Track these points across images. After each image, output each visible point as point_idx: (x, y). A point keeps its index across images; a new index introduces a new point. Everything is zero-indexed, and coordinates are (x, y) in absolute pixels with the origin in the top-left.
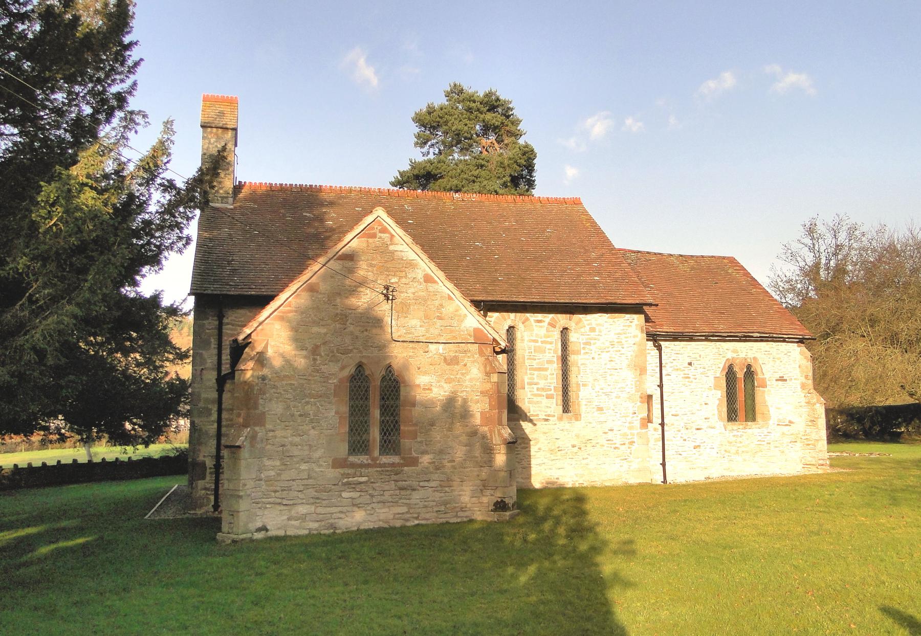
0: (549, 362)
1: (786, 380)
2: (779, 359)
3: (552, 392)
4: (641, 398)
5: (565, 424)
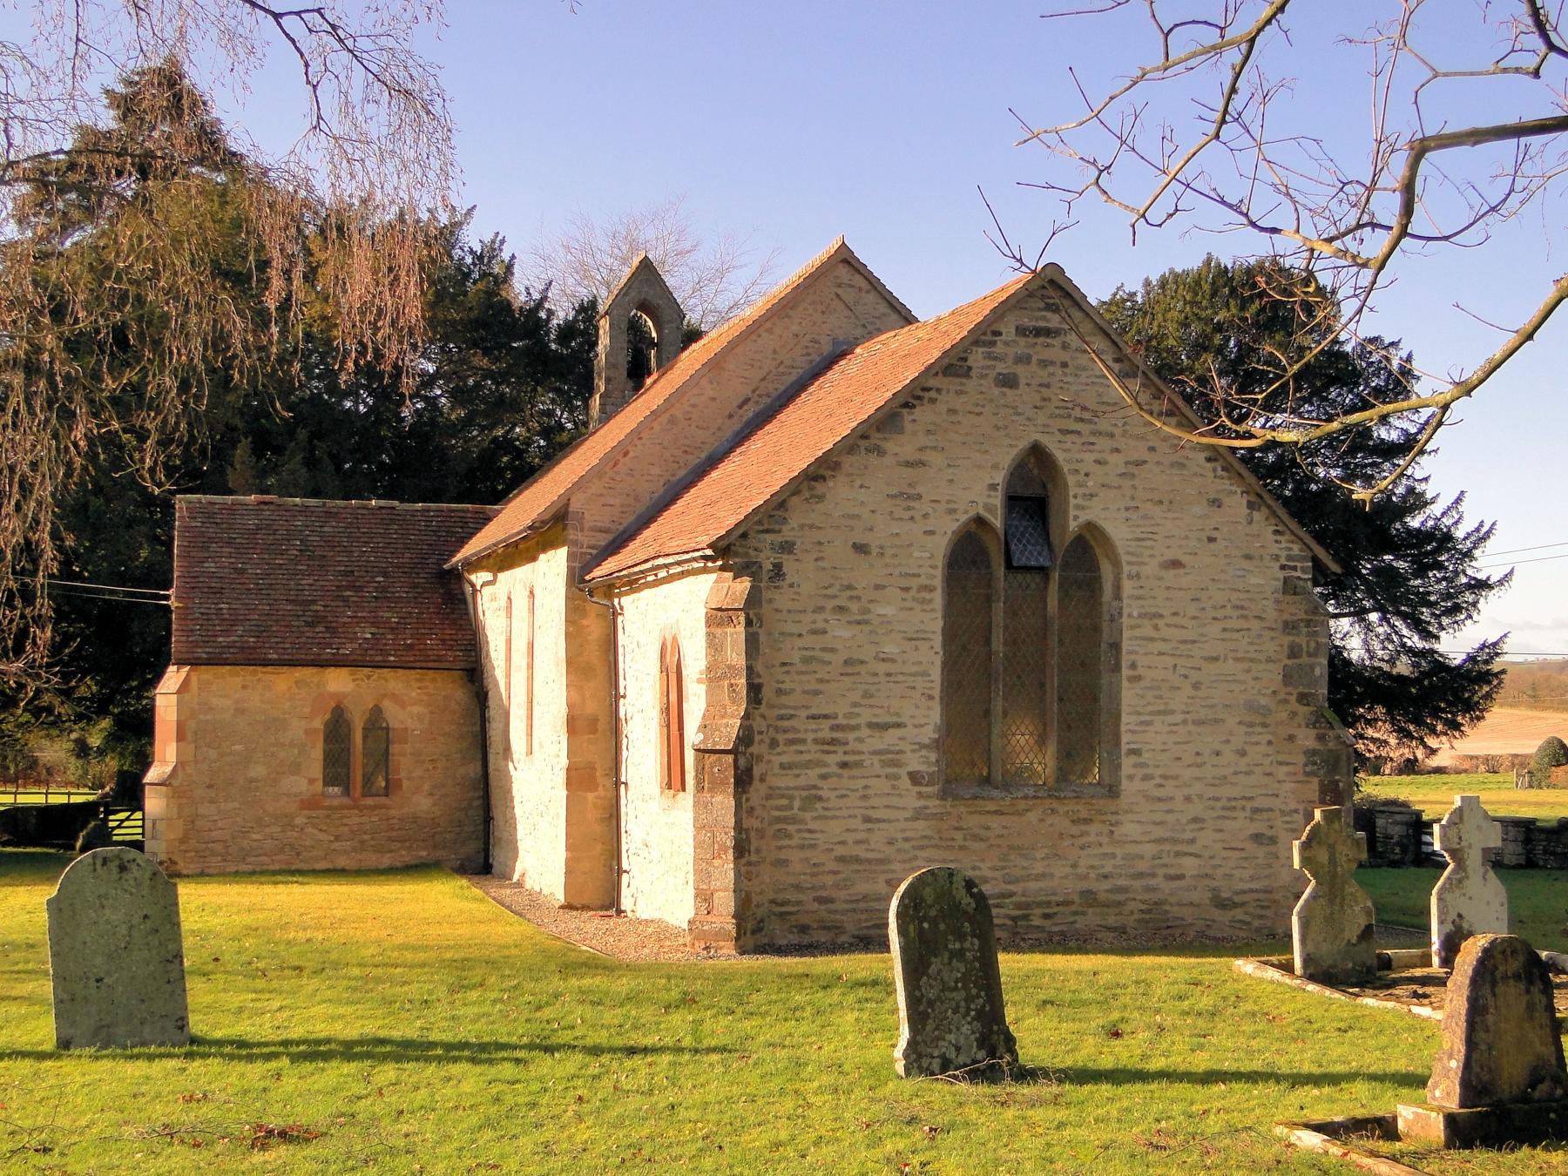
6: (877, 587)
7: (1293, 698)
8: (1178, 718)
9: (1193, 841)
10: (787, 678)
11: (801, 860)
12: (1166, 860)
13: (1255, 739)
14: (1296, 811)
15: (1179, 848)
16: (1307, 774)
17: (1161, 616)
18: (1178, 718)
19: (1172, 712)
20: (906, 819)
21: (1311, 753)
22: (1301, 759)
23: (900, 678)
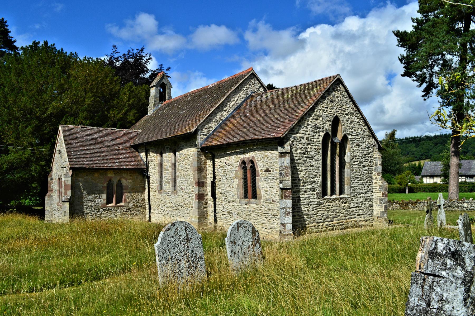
0: (170, 167)
1: (270, 171)
2: (266, 156)
3: (170, 181)
4: (196, 183)
5: (173, 196)
6: (311, 148)
7: (376, 174)
8: (359, 179)
9: (361, 207)
10: (294, 170)
11: (297, 215)
12: (357, 211)
13: (370, 183)
14: (377, 199)
15: (359, 208)
16: (379, 191)
17: (356, 156)
18: (359, 179)
19: (358, 178)
20: (316, 204)
21: (380, 186)
22: (378, 187)
23: (315, 170)
